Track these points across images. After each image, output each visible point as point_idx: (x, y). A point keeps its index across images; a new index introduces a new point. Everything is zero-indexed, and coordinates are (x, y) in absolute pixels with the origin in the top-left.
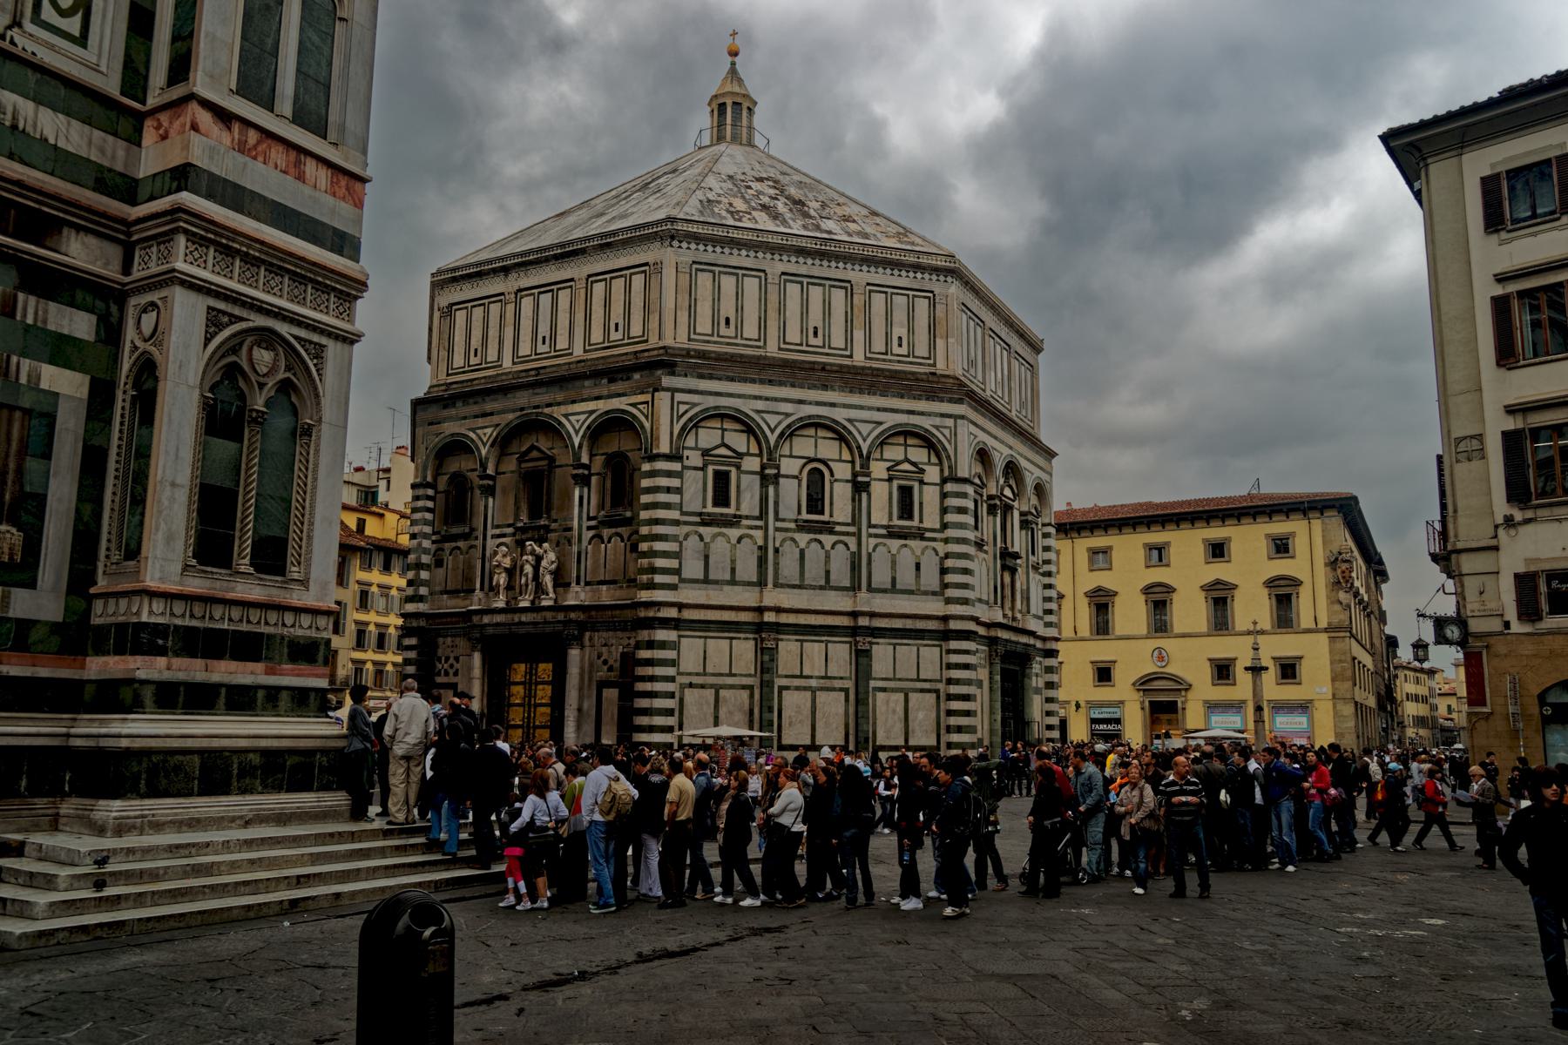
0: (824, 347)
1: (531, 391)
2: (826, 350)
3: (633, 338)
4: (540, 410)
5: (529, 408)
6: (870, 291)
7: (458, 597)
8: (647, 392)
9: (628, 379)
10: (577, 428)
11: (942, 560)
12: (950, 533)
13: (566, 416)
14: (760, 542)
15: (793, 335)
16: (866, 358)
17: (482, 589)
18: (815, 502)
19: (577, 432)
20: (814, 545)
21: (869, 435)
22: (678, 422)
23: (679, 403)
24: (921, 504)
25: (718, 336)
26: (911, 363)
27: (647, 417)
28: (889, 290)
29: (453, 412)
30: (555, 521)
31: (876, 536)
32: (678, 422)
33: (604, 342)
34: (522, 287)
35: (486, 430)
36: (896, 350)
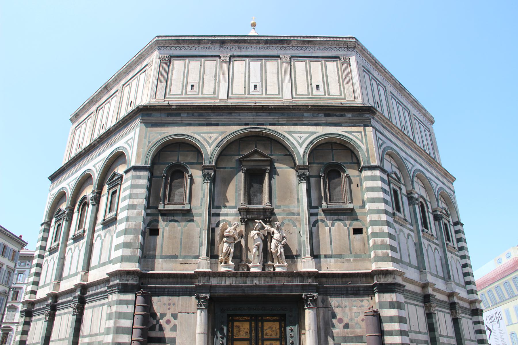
1: (254, 113)
3: (333, 95)
4: (264, 127)
5: (254, 124)
7: (176, 261)
8: (359, 126)
9: (342, 116)
10: (301, 141)
13: (289, 133)
17: (207, 255)
19: (301, 145)
20: (429, 247)
24: (451, 234)
27: (362, 142)
29: (178, 119)
30: (279, 207)
33: (308, 94)
34: (235, 54)
35: (211, 135)
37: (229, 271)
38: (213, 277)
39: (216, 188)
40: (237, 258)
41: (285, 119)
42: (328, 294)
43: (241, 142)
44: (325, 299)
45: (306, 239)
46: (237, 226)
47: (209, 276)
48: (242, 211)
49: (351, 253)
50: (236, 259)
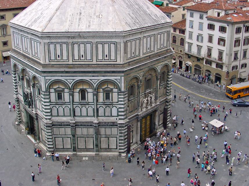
0: (85, 60)
2: (86, 60)
6: (98, 44)
11: (118, 109)
12: (120, 103)
14: (70, 108)
15: (76, 57)
16: (97, 61)
18: (83, 97)
21: (96, 82)
22: (47, 83)
23: (46, 79)
25: (57, 60)
26: (109, 61)
28: (103, 43)
31: (100, 104)
32: (47, 83)
36: (105, 58)
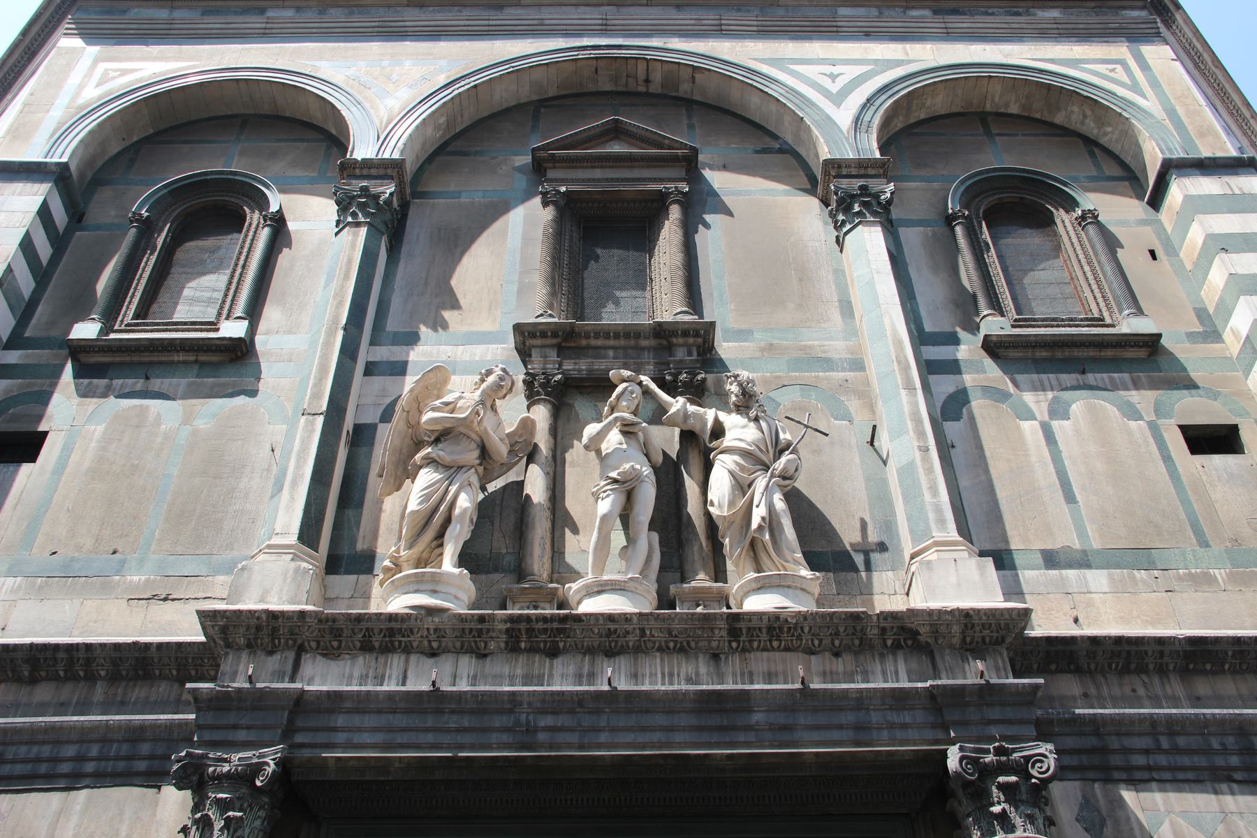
10: (834, 88)
27: (1135, 87)
37: (431, 611)
38: (324, 655)
39: (402, 265)
40: (496, 570)
41: (755, 23)
42: (1116, 775)
43: (543, 110)
44: (1102, 802)
45: (918, 455)
46: (501, 379)
47: (300, 650)
48: (538, 342)
49: (1204, 543)
50: (487, 572)
